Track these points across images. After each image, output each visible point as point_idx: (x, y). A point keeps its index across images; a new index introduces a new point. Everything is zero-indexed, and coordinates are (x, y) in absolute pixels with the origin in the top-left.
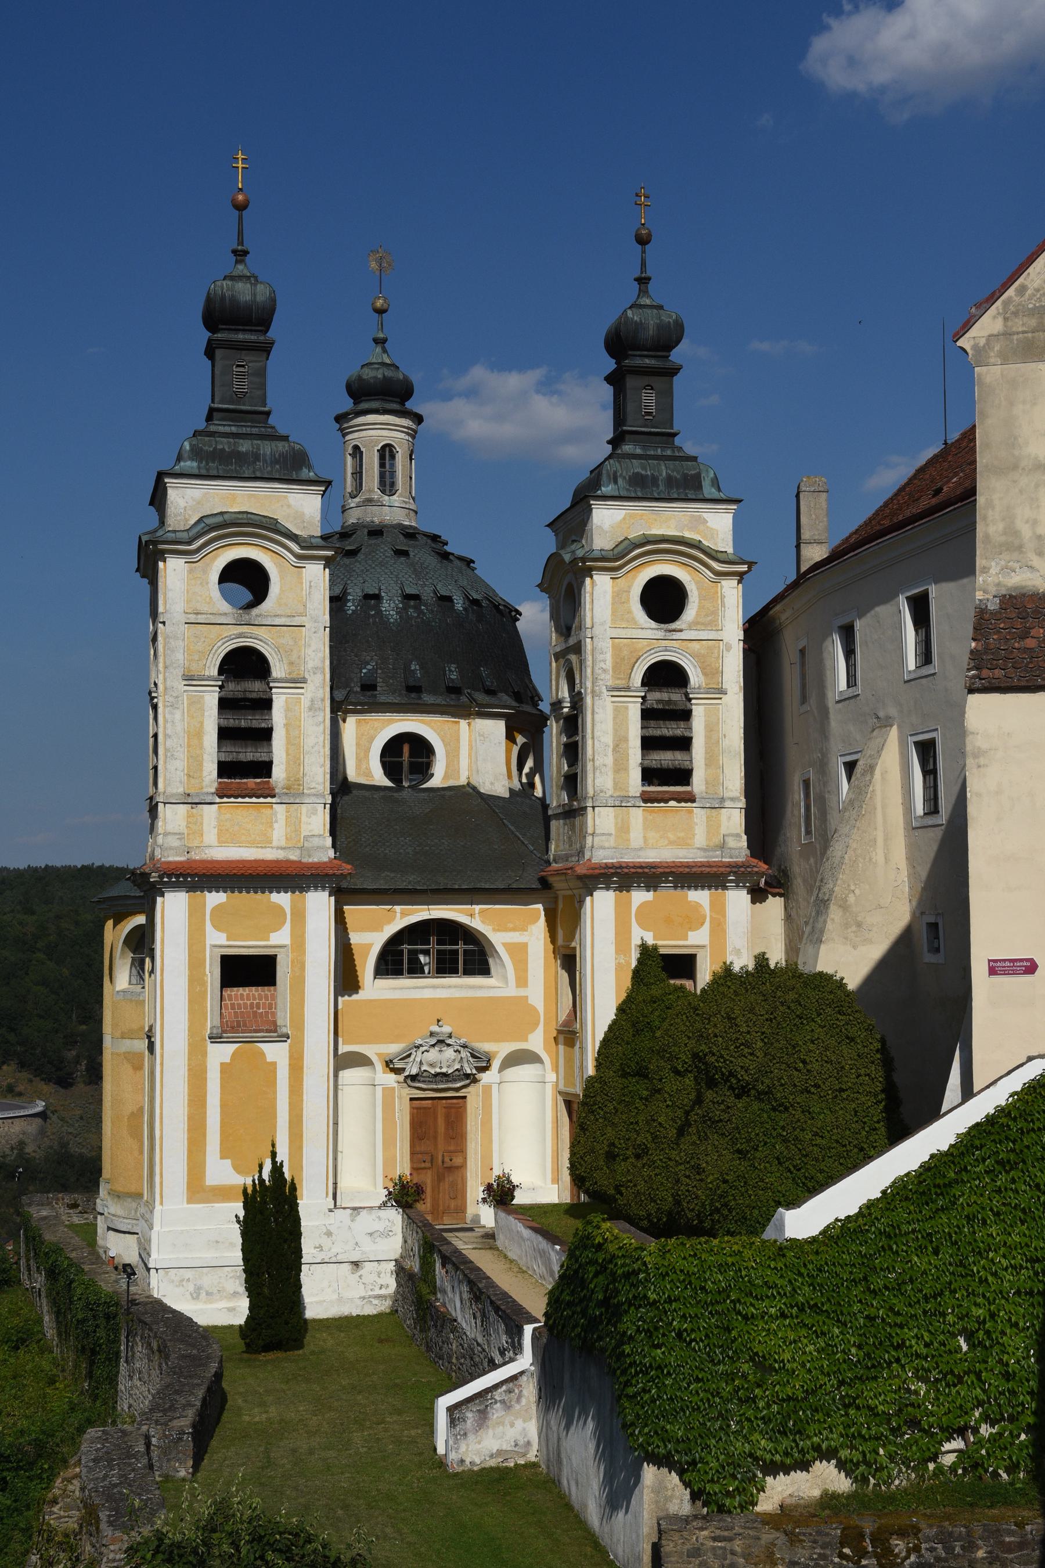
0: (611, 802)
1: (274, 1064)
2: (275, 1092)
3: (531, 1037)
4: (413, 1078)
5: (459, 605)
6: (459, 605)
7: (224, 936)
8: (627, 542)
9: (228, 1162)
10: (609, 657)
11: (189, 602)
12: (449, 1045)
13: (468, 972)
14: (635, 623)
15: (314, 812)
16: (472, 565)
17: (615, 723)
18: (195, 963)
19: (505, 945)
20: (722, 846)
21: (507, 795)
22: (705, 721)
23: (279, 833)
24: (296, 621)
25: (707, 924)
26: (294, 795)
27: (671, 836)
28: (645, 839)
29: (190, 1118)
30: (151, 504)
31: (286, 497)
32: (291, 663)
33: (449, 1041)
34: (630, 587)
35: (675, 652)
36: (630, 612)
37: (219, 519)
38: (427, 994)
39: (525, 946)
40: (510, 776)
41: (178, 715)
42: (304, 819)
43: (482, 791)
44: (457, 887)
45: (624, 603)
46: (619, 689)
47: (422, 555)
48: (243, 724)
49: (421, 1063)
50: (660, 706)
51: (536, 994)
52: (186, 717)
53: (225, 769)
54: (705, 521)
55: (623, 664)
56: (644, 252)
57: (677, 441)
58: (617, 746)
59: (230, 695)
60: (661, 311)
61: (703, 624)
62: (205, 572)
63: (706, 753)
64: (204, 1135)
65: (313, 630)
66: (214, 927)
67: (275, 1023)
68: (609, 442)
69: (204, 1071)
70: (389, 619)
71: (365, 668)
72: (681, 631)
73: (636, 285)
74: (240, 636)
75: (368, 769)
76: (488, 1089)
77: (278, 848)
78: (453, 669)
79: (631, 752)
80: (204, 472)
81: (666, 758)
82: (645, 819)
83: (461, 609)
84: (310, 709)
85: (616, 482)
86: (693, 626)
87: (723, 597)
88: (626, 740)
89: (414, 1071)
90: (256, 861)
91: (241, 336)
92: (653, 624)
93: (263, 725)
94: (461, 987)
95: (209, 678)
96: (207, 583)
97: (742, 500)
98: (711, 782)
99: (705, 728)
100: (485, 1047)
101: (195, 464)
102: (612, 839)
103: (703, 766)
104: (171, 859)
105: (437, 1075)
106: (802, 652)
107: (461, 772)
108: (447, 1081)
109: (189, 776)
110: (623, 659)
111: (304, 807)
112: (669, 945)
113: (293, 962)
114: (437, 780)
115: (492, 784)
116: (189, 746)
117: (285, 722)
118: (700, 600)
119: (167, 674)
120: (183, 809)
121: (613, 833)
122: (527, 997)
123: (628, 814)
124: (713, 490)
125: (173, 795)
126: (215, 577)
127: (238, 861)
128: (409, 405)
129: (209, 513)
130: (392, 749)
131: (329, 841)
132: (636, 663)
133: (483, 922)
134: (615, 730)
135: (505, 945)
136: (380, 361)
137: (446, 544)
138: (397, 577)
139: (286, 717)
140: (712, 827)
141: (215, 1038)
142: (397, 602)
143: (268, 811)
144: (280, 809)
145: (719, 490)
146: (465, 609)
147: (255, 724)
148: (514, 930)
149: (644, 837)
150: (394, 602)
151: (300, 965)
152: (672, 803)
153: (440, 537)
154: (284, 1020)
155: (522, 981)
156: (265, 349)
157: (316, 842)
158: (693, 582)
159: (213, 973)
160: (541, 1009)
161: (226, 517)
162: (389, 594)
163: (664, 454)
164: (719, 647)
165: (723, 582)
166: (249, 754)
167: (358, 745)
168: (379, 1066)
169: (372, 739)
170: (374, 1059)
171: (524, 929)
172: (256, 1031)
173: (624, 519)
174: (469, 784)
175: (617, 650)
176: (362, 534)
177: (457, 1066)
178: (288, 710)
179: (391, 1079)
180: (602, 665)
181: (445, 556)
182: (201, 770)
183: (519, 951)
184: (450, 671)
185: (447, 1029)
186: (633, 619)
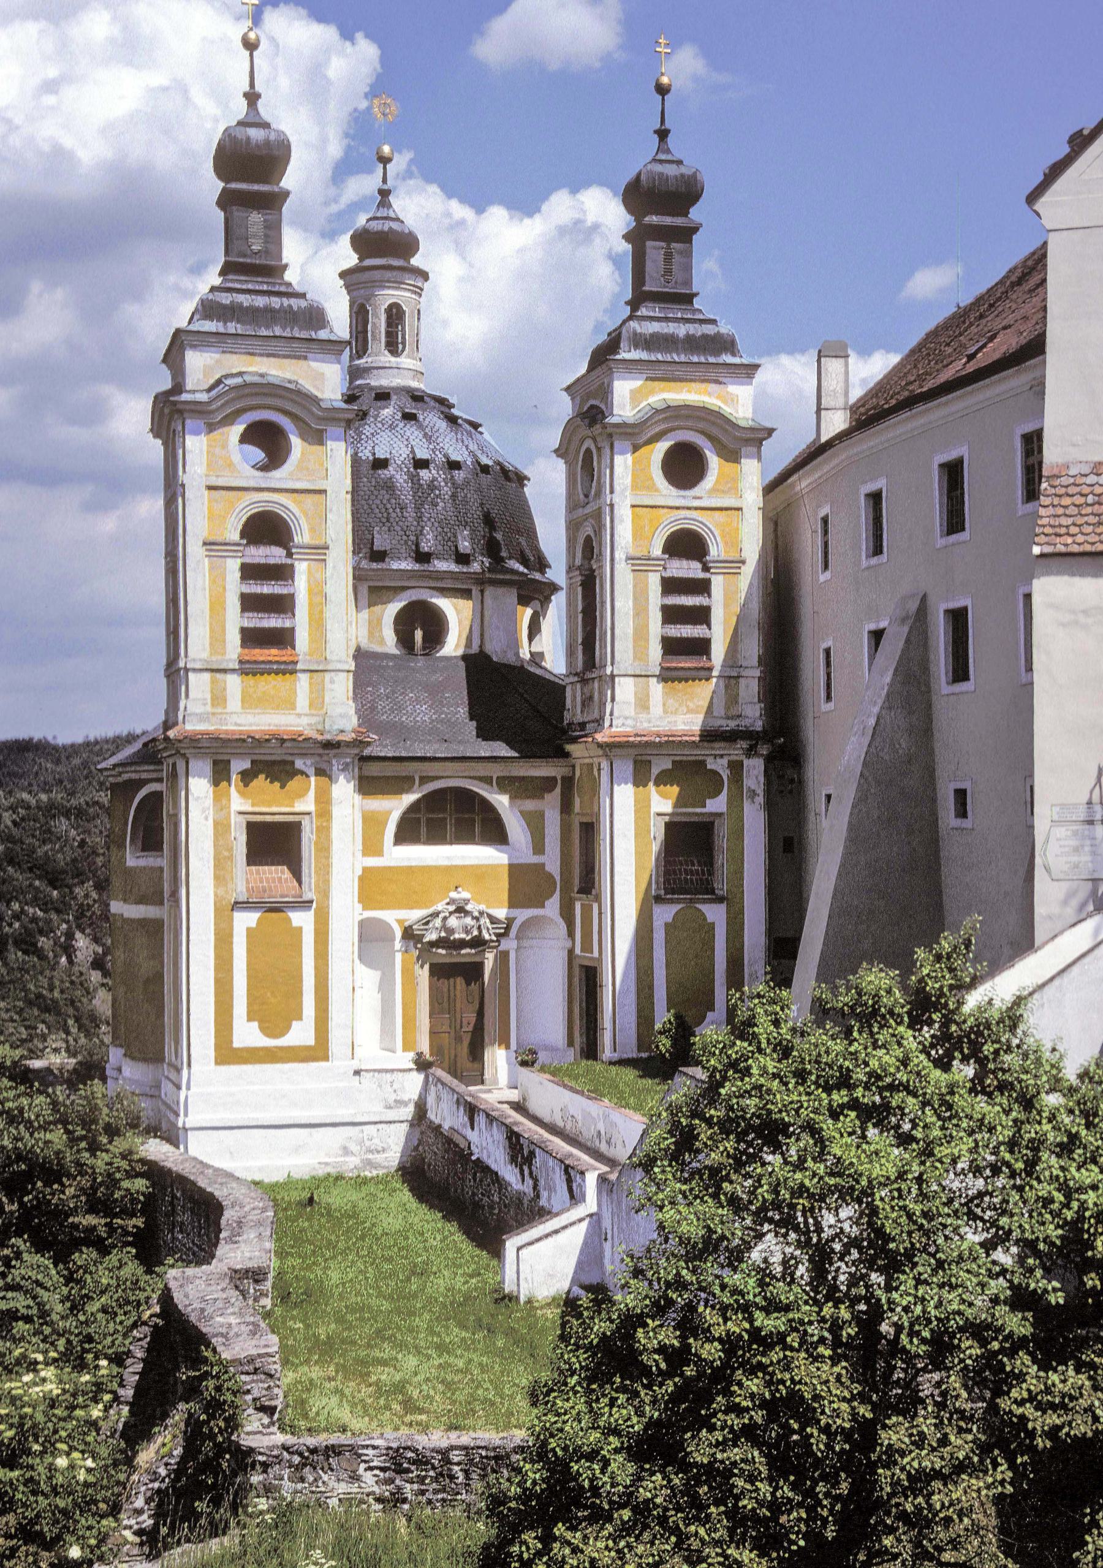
1: (300, 929)
9: (256, 1024)
14: (657, 490)
18: (221, 828)
30: (165, 360)
33: (469, 908)
42: (328, 685)
47: (433, 419)
57: (697, 303)
68: (627, 303)
73: (656, 138)
86: (714, 491)
92: (673, 491)
106: (825, 520)
120: (207, 676)
122: (543, 865)
128: (415, 261)
137: (453, 406)
156: (686, 234)
161: (248, 379)
166: (273, 622)
177: (475, 933)
181: (452, 420)
185: (465, 895)
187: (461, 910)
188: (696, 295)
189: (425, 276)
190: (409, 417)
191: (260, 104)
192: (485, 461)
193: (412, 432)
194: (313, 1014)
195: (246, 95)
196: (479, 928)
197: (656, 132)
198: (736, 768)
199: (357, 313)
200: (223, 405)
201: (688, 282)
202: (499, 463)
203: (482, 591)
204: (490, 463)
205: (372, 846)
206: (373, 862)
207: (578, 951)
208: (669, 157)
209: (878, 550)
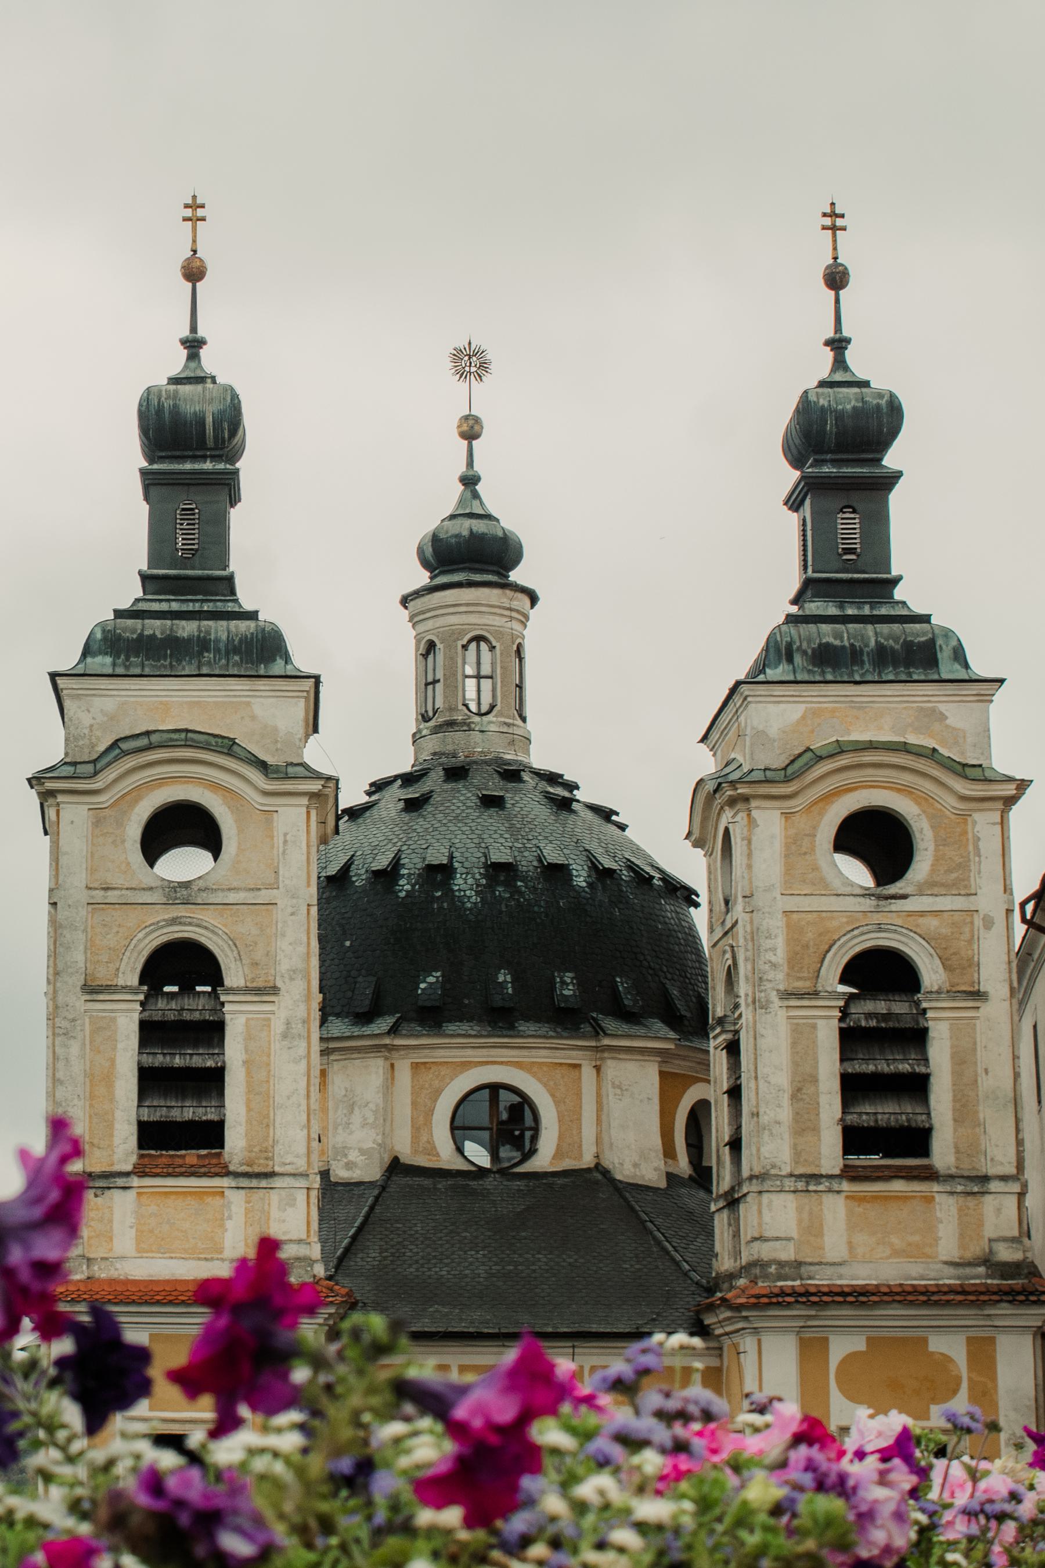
5: (581, 878)
6: (581, 878)
8: (809, 755)
10: (780, 941)
11: (92, 870)
16: (614, 818)
21: (663, 1184)
22: (952, 1047)
24: (264, 896)
27: (895, 1240)
28: (850, 1245)
31: (248, 704)
34: (815, 828)
35: (895, 931)
36: (816, 868)
40: (669, 1152)
43: (619, 1177)
44: (550, 1330)
45: (805, 854)
46: (800, 996)
48: (178, 1061)
50: (873, 1023)
52: (88, 1050)
54: (943, 717)
56: (837, 301)
57: (899, 593)
58: (799, 1090)
59: (157, 1017)
60: (864, 390)
61: (942, 885)
62: (120, 824)
63: (955, 1100)
65: (290, 910)
70: (464, 903)
71: (425, 982)
72: (904, 897)
74: (174, 921)
75: (430, 1142)
78: (569, 980)
79: (823, 1100)
82: (850, 1213)
83: (584, 884)
84: (285, 1036)
85: (790, 660)
88: (814, 1080)
93: (210, 1063)
95: (125, 989)
96: (123, 841)
97: (1001, 681)
98: (968, 1148)
99: (952, 1058)
103: (951, 1122)
107: (584, 1147)
115: (636, 1165)
117: (244, 1057)
118: (936, 846)
119: (58, 984)
121: (794, 1234)
123: (821, 1204)
124: (957, 666)
128: (514, 576)
132: (828, 951)
134: (796, 1064)
136: (467, 511)
137: (577, 788)
138: (480, 837)
139: (246, 1051)
140: (968, 1227)
142: (478, 876)
146: (590, 885)
147: (197, 1062)
149: (850, 1243)
150: (473, 878)
152: (898, 1186)
153: (561, 776)
158: (923, 817)
162: (466, 864)
163: (875, 613)
164: (972, 923)
165: (976, 816)
166: (188, 1111)
167: (414, 1104)
169: (437, 1093)
173: (803, 718)
176: (436, 776)
178: (249, 1037)
180: (770, 956)
184: (563, 983)
186: (822, 880)
190: (492, 802)
192: (608, 863)
193: (491, 819)
197: (828, 343)
199: (425, 656)
200: (115, 781)
201: (885, 562)
202: (631, 867)
203: (598, 1069)
204: (614, 866)
208: (846, 378)
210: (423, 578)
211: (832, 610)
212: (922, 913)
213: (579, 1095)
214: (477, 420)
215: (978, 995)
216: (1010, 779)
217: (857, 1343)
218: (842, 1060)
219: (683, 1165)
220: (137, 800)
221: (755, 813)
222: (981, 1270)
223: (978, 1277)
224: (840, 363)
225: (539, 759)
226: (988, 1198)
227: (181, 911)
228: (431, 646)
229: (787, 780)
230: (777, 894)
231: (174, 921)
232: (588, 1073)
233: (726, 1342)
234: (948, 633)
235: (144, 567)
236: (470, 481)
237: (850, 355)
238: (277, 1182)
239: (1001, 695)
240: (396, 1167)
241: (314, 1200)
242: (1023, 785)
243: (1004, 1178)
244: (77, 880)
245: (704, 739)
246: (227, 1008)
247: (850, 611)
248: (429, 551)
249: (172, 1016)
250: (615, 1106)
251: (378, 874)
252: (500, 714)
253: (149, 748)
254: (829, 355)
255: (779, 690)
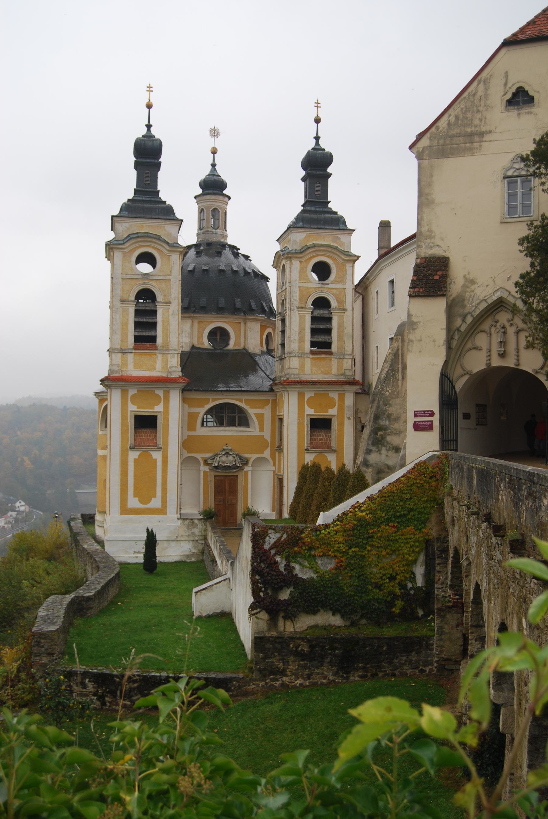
0: (297, 355)
2: (156, 471)
3: (265, 452)
4: (216, 468)
6: (242, 273)
7: (136, 407)
10: (297, 295)
11: (123, 269)
12: (230, 455)
13: (240, 425)
14: (309, 281)
15: (174, 357)
17: (300, 322)
19: (255, 414)
20: (344, 374)
21: (260, 353)
23: (159, 365)
24: (168, 278)
25: (336, 406)
26: (166, 350)
29: (121, 480)
30: (112, 230)
32: (165, 296)
34: (307, 266)
36: (307, 276)
37: (136, 235)
38: (222, 433)
39: (263, 414)
40: (262, 346)
41: (118, 316)
42: (169, 360)
46: (302, 308)
48: (145, 320)
49: (219, 462)
51: (267, 435)
53: (137, 339)
55: (303, 298)
57: (330, 205)
64: (127, 487)
66: (132, 403)
67: (156, 443)
68: (302, 206)
69: (127, 462)
72: (328, 284)
74: (144, 284)
75: (202, 341)
76: (247, 473)
77: (158, 371)
79: (306, 334)
80: (130, 215)
81: (320, 338)
82: (311, 363)
87: (346, 270)
88: (304, 329)
89: (216, 465)
90: (149, 377)
91: (148, 160)
94: (237, 431)
97: (354, 230)
100: (247, 456)
101: (127, 213)
102: (297, 371)
104: (114, 375)
105: (226, 466)
106: (377, 292)
108: (230, 469)
109: (122, 341)
110: (304, 296)
111: (169, 355)
112: (321, 414)
113: (164, 418)
114: (231, 346)
115: (254, 348)
116: (122, 328)
120: (119, 355)
125: (115, 349)
126: (134, 259)
127: (142, 377)
128: (225, 192)
129: (132, 233)
130: (213, 334)
131: (180, 369)
133: (246, 405)
134: (300, 325)
135: (255, 414)
137: (239, 249)
140: (340, 366)
141: (132, 448)
143: (155, 356)
144: (160, 356)
145: (346, 226)
147: (150, 320)
148: (259, 408)
151: (167, 420)
154: (160, 441)
155: (262, 429)
157: (174, 369)
159: (131, 422)
160: (269, 441)
166: (148, 333)
167: (198, 331)
168: (202, 464)
170: (200, 460)
171: (263, 407)
172: (148, 446)
173: (305, 237)
174: (244, 349)
175: (300, 291)
177: (234, 463)
178: (163, 314)
179: (207, 468)
180: (295, 298)
182: (127, 339)
183: (260, 417)
185: (230, 448)
186: (308, 279)
187: (227, 454)
188: (330, 202)
189: (229, 198)
191: (152, 129)
192: (249, 271)
194: (161, 495)
195: (146, 126)
196: (235, 461)
197: (314, 138)
198: (341, 397)
199: (201, 212)
200: (129, 246)
202: (254, 271)
203: (245, 323)
205: (191, 426)
206: (192, 433)
207: (277, 472)
209: (393, 305)
210: (200, 191)
211: (313, 209)
212: (332, 288)
213: (240, 330)
214: (216, 149)
215: (345, 310)
216: (355, 256)
217: (312, 394)
218: (311, 324)
219: (265, 349)
220: (134, 251)
221: (293, 261)
222: (342, 377)
223: (342, 378)
224: (317, 143)
225: (230, 241)
226: (344, 360)
227: (146, 281)
228: (202, 210)
229: (301, 253)
230: (297, 282)
231: (144, 284)
232: (242, 325)
233: (278, 394)
234: (342, 217)
235: (135, 187)
236: (214, 165)
237: (320, 141)
238: (170, 352)
239: (354, 232)
240: (193, 347)
241: (179, 357)
242: (358, 257)
243: (349, 355)
244: (119, 271)
245: (277, 240)
246: (158, 307)
247: (318, 209)
248: (202, 184)
249: (143, 308)
250: (249, 333)
251: (190, 271)
252: (220, 229)
253: (138, 237)
254: (314, 141)
255: (300, 230)
